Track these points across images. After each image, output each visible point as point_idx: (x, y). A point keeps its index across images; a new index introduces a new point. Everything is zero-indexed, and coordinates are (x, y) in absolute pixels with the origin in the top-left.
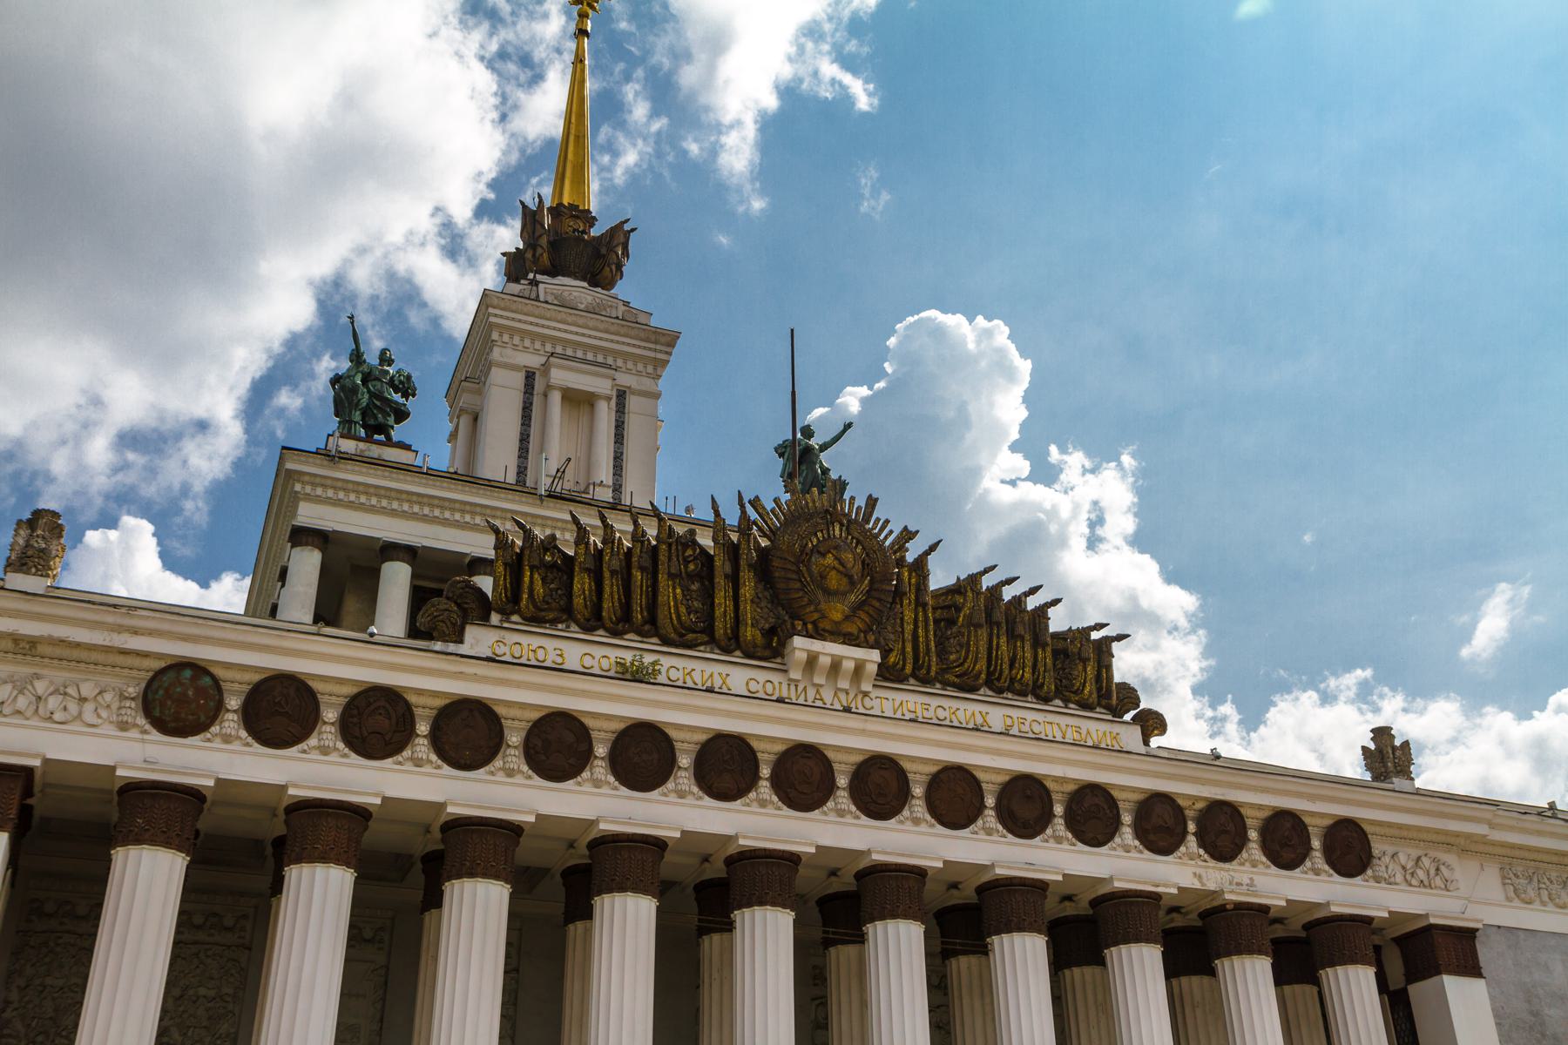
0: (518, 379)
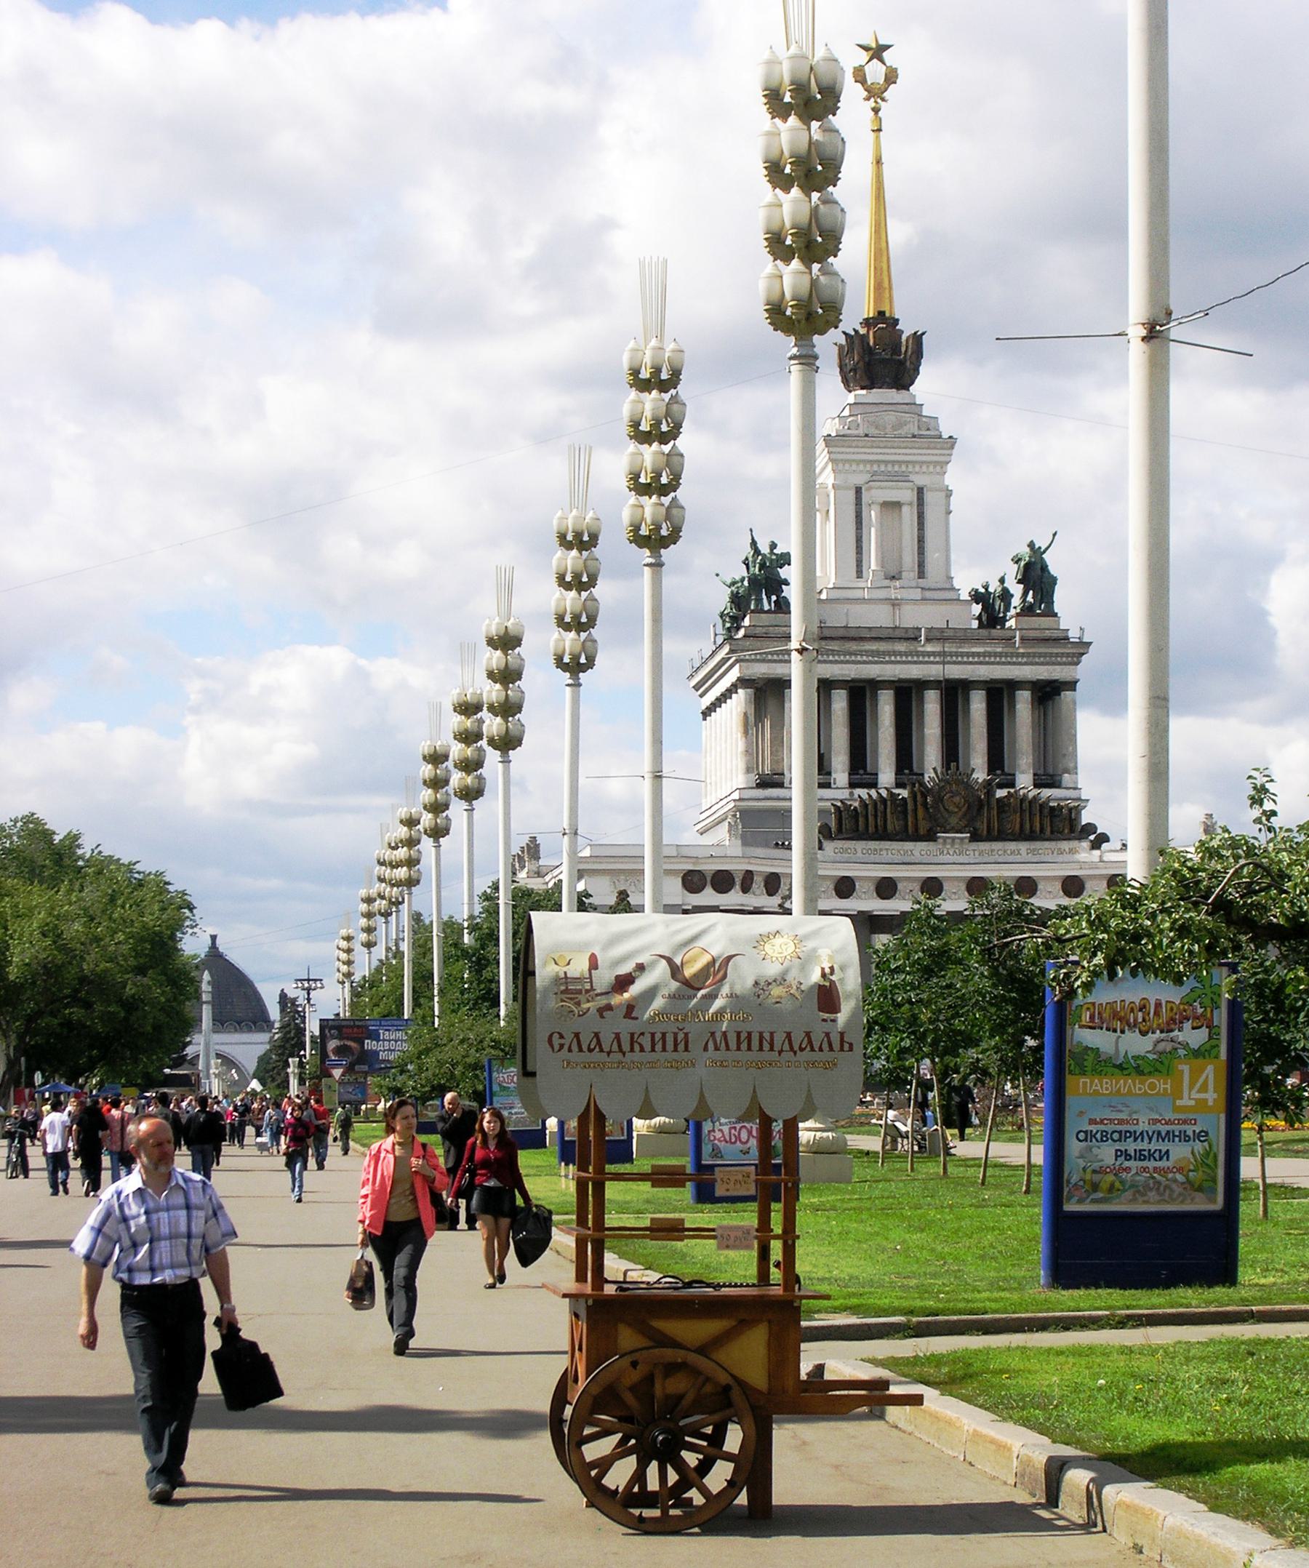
0: (852, 494)
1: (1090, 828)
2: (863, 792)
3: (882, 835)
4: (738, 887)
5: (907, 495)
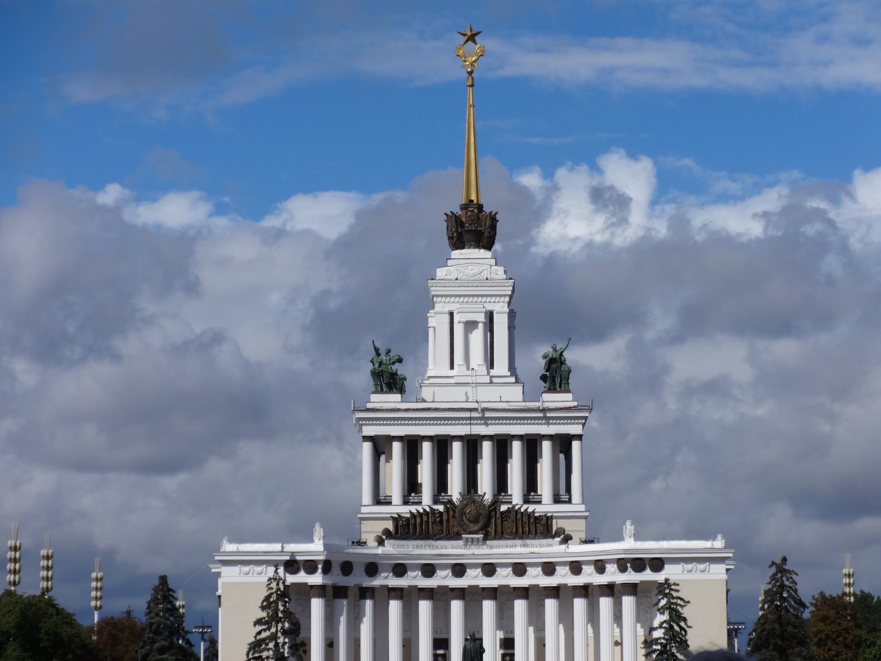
0: (447, 318)
1: (560, 532)
2: (413, 509)
4: (320, 570)
5: (481, 318)
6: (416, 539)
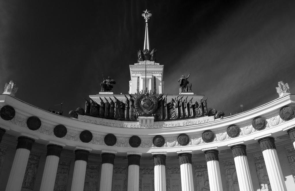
0: (137, 78)
3: (110, 117)
5: (151, 77)
6: (103, 118)
